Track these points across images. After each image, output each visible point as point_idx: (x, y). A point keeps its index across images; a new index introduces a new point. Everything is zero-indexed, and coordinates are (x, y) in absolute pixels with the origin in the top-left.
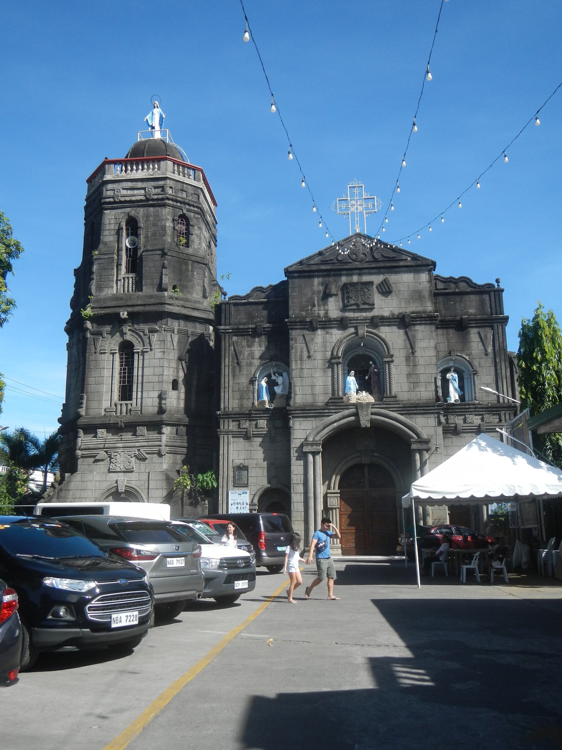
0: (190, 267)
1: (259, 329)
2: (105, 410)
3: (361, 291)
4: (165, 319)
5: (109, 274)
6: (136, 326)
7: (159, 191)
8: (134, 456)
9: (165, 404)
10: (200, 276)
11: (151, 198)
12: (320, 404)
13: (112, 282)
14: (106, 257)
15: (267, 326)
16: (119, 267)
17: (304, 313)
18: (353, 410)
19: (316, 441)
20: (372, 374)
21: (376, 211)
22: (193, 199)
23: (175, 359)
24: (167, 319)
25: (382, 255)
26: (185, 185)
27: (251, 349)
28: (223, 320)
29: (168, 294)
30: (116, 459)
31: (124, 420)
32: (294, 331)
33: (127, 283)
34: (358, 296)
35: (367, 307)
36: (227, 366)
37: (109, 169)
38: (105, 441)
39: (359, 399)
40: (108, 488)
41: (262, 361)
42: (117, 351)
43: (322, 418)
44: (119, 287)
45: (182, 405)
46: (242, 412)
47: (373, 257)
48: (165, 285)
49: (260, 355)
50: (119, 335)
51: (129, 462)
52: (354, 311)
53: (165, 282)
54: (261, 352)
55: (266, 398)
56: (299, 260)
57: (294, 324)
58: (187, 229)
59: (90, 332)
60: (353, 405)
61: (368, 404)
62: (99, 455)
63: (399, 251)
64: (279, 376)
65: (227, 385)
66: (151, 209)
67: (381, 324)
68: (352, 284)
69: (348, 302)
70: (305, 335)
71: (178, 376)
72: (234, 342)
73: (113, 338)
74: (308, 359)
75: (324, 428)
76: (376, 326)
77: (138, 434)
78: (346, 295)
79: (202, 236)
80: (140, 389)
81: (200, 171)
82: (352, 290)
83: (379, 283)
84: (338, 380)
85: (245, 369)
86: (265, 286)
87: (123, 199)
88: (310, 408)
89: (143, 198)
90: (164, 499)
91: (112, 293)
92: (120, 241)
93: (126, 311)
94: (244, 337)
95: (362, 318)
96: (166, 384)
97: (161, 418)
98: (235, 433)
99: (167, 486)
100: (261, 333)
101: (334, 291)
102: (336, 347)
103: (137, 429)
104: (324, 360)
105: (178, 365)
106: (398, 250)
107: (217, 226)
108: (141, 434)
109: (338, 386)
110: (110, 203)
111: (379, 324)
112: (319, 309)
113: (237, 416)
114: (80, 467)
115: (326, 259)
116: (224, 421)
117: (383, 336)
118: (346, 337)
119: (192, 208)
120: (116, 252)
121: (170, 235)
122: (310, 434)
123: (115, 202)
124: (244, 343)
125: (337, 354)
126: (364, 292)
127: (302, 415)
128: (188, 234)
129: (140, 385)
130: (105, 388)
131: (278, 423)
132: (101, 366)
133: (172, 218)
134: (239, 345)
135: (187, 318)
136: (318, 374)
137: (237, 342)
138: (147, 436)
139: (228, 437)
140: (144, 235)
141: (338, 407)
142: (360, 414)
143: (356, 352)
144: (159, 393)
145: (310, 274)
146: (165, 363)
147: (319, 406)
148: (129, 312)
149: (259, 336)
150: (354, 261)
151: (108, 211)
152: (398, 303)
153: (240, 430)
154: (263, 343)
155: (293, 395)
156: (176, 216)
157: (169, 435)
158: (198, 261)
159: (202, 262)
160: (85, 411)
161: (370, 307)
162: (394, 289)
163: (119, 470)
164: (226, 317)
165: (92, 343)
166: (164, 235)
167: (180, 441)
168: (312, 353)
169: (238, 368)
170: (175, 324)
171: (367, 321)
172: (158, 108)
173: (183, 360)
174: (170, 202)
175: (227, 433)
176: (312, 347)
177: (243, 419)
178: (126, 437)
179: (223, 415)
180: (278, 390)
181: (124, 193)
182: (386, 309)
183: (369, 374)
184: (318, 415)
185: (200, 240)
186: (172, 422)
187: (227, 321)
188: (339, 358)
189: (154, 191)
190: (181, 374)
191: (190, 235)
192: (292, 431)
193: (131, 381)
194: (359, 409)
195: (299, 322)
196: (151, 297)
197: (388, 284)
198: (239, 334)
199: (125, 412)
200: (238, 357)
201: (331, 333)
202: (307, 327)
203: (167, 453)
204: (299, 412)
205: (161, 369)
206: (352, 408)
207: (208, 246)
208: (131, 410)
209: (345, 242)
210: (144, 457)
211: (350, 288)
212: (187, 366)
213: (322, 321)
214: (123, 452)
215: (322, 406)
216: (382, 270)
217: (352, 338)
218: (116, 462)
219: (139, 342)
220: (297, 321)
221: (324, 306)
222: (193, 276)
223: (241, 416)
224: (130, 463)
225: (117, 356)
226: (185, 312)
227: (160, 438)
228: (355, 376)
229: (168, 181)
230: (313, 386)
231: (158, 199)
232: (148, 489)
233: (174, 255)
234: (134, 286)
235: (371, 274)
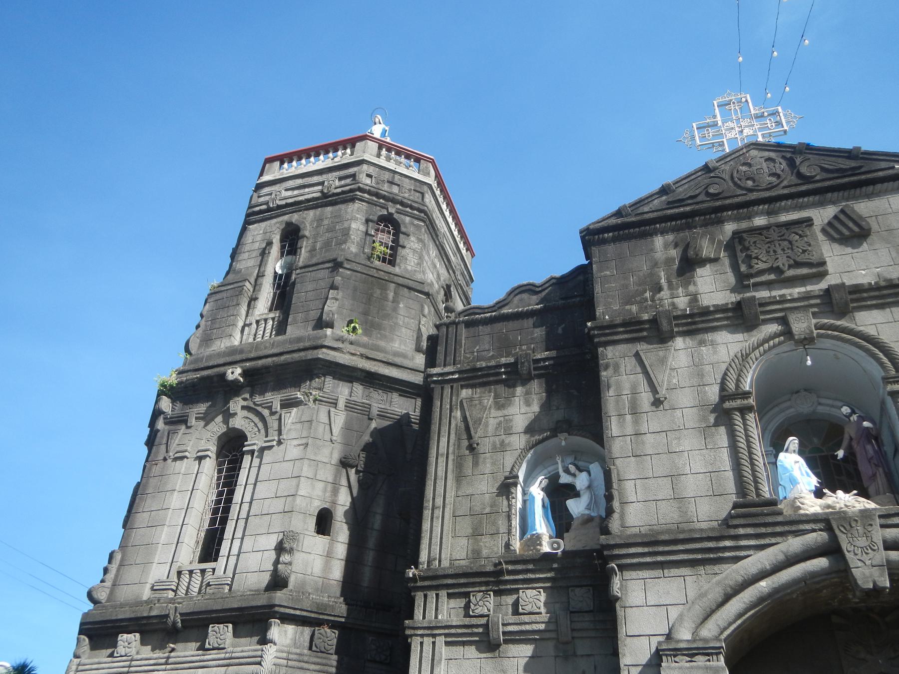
0: (391, 295)
1: (523, 363)
2: (152, 589)
3: (781, 240)
4: (319, 377)
5: (229, 314)
6: (258, 399)
7: (348, 181)
9: (290, 563)
10: (413, 312)
11: (330, 193)
12: (704, 525)
13: (231, 327)
14: (232, 286)
15: (543, 357)
16: (253, 302)
17: (634, 308)
18: (817, 537)
19: (705, 640)
20: (854, 444)
21: (786, 128)
22: (411, 198)
23: (333, 462)
24: (323, 378)
25: (823, 169)
26: (397, 177)
27: (506, 412)
28: (440, 357)
29: (333, 333)
31: (184, 608)
32: (610, 348)
33: (262, 329)
34: (775, 251)
35: (805, 271)
36: (442, 455)
37: (269, 169)
38: (130, 666)
39: (829, 507)
41: (532, 436)
42: (214, 456)
43: (716, 568)
44: (245, 337)
45: (337, 572)
46: (475, 570)
47: (800, 175)
48: (328, 314)
49: (527, 423)
50: (221, 420)
52: (769, 285)
53: (330, 309)
54: (531, 416)
55: (542, 526)
56: (615, 208)
57: (607, 331)
58: (396, 241)
59: (164, 419)
60: (814, 519)
61: (865, 514)
63: (865, 156)
64: (577, 472)
65: (439, 501)
66: (329, 209)
67: (855, 305)
68: (755, 230)
69: (751, 267)
70: (641, 353)
71: (334, 503)
72: (464, 401)
73: (207, 428)
74: (654, 408)
75: (727, 598)
76: (844, 312)
77: (209, 644)
78: (741, 256)
79: (426, 258)
80: (239, 534)
81: (430, 162)
82: (755, 242)
83: (826, 221)
84: (750, 453)
85: (488, 461)
86: (539, 278)
87: (283, 202)
88: (672, 537)
89: (319, 195)
91: (228, 345)
92: (263, 264)
93: (241, 367)
94: (488, 388)
95: (796, 296)
96: (301, 516)
97: (270, 598)
98: (453, 631)
100: (530, 369)
101: (707, 249)
102: (732, 371)
103: (210, 629)
104: (702, 406)
105: (337, 476)
106: (861, 156)
107: (472, 285)
108: (216, 645)
109: (754, 471)
110: (261, 212)
111: (852, 305)
112: (672, 294)
113: (462, 581)
115: (680, 197)
116: (425, 596)
117: (871, 331)
118: (758, 347)
119: (408, 209)
120: (252, 281)
121: (358, 242)
122: (681, 617)
123: (269, 210)
124: (489, 400)
125: (737, 386)
126: (790, 242)
127: (648, 559)
128: (396, 246)
129: (241, 523)
130: (165, 535)
131: (581, 597)
132: (169, 487)
133: (364, 219)
134: (476, 405)
135: (371, 380)
136: (689, 442)
137: (471, 399)
138: (229, 650)
139: (434, 643)
140: (309, 248)
141: (763, 530)
142: (844, 545)
143: (792, 410)
144: (280, 539)
145: (643, 228)
146: (305, 469)
147: (702, 530)
148: (245, 368)
149: (525, 380)
150: (750, 190)
151: (255, 225)
152: (894, 254)
153: (467, 621)
154: (534, 396)
155: (616, 504)
156: (373, 215)
157: (286, 649)
158: (410, 285)
159: (419, 288)
160: (108, 591)
161: (814, 270)
162: (874, 226)
164: (448, 349)
165: (164, 441)
166: (345, 242)
167: (317, 667)
168: (662, 392)
169: (469, 461)
170: (343, 391)
171: (813, 302)
172: (380, 123)
173: (352, 467)
174: (366, 195)
175: (432, 630)
176: (662, 379)
177: (477, 589)
178: (182, 654)
179: (423, 579)
180: (576, 507)
181: (283, 194)
182: (863, 272)
183: (845, 443)
184: (699, 556)
185: (421, 258)
186: (298, 613)
187: (450, 359)
188: (746, 395)
189: (337, 183)
190: (344, 500)
191: (399, 248)
192: (620, 612)
193: (224, 521)
194: (837, 532)
195: (624, 324)
196: (299, 340)
197: (854, 217)
198: (477, 381)
199: (197, 590)
200: (472, 433)
201: (712, 341)
202: (645, 334)
204: (640, 550)
205: (295, 481)
206: (814, 531)
207: (443, 287)
208: (208, 585)
209: (723, 162)
211: (749, 240)
212: (359, 481)
213: (685, 316)
215: (712, 529)
216: (829, 195)
217: (774, 346)
219: (259, 430)
220: (617, 322)
221: (686, 285)
222: (395, 309)
223: (472, 580)
225: (210, 466)
226: (366, 365)
227: (259, 653)
228: (801, 453)
229: (365, 167)
230: (674, 477)
231: (343, 193)
233: (359, 269)
234: (274, 333)
235: (802, 207)
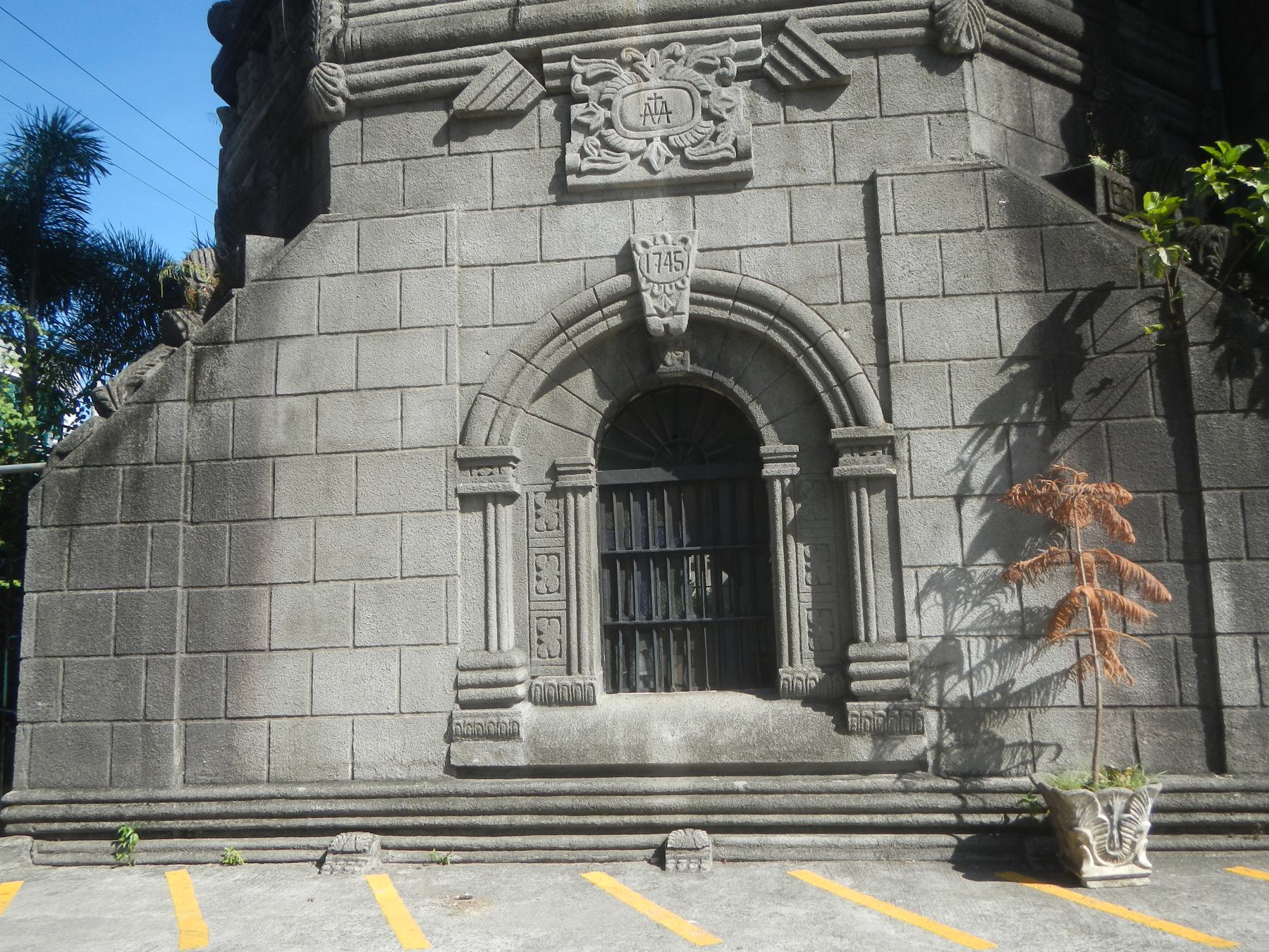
8: (742, 75)
30: (607, 104)
40: (563, 312)
51: (707, 114)
62: (476, 84)
90: (1015, 369)
99: (1025, 274)
114: (349, 177)
163: (640, 174)
203: (987, 49)
210: (823, 74)
214: (660, 46)
218: (609, 123)
224: (719, 120)
232: (878, 299)
